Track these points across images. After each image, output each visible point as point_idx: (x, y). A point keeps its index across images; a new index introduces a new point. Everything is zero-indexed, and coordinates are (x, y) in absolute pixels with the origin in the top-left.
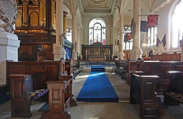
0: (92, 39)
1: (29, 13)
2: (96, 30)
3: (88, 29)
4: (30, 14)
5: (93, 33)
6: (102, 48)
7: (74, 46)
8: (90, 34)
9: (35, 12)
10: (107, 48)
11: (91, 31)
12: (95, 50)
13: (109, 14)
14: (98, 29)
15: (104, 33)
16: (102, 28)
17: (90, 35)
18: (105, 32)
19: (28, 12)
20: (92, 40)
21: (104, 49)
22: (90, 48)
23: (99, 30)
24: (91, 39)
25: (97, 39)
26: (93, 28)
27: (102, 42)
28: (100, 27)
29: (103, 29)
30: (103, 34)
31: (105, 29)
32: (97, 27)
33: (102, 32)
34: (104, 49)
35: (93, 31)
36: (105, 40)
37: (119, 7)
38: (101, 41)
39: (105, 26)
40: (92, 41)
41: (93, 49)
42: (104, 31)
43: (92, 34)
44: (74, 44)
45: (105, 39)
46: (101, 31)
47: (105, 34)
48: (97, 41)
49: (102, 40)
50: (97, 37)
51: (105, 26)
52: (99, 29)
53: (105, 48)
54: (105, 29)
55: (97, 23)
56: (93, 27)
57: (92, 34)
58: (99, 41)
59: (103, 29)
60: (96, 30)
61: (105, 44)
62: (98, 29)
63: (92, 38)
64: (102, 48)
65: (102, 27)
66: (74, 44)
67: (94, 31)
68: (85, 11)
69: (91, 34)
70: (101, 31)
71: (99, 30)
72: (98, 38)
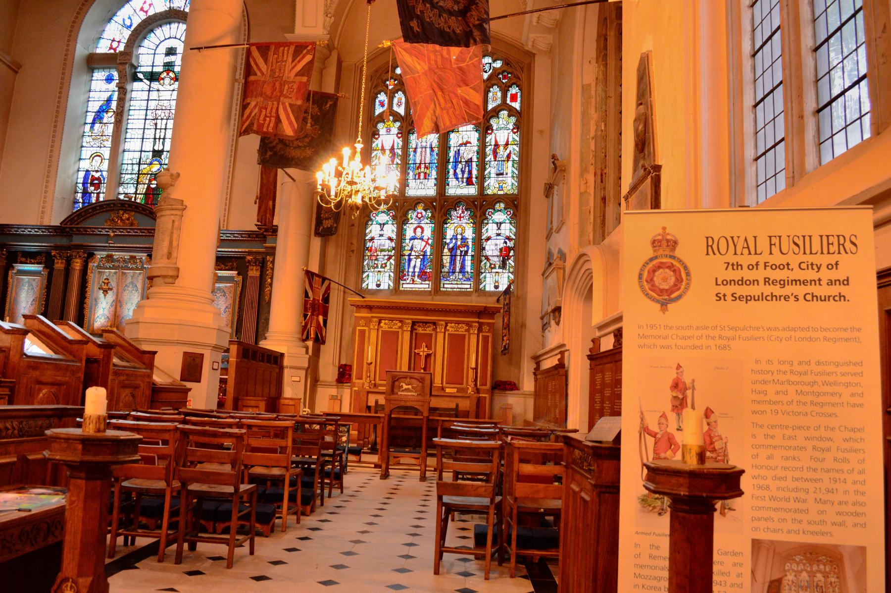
0: (105, 166)
2: (153, 77)
5: (114, 105)
14: (169, 67)
35: (122, 90)
63: (106, 153)
69: (98, 117)
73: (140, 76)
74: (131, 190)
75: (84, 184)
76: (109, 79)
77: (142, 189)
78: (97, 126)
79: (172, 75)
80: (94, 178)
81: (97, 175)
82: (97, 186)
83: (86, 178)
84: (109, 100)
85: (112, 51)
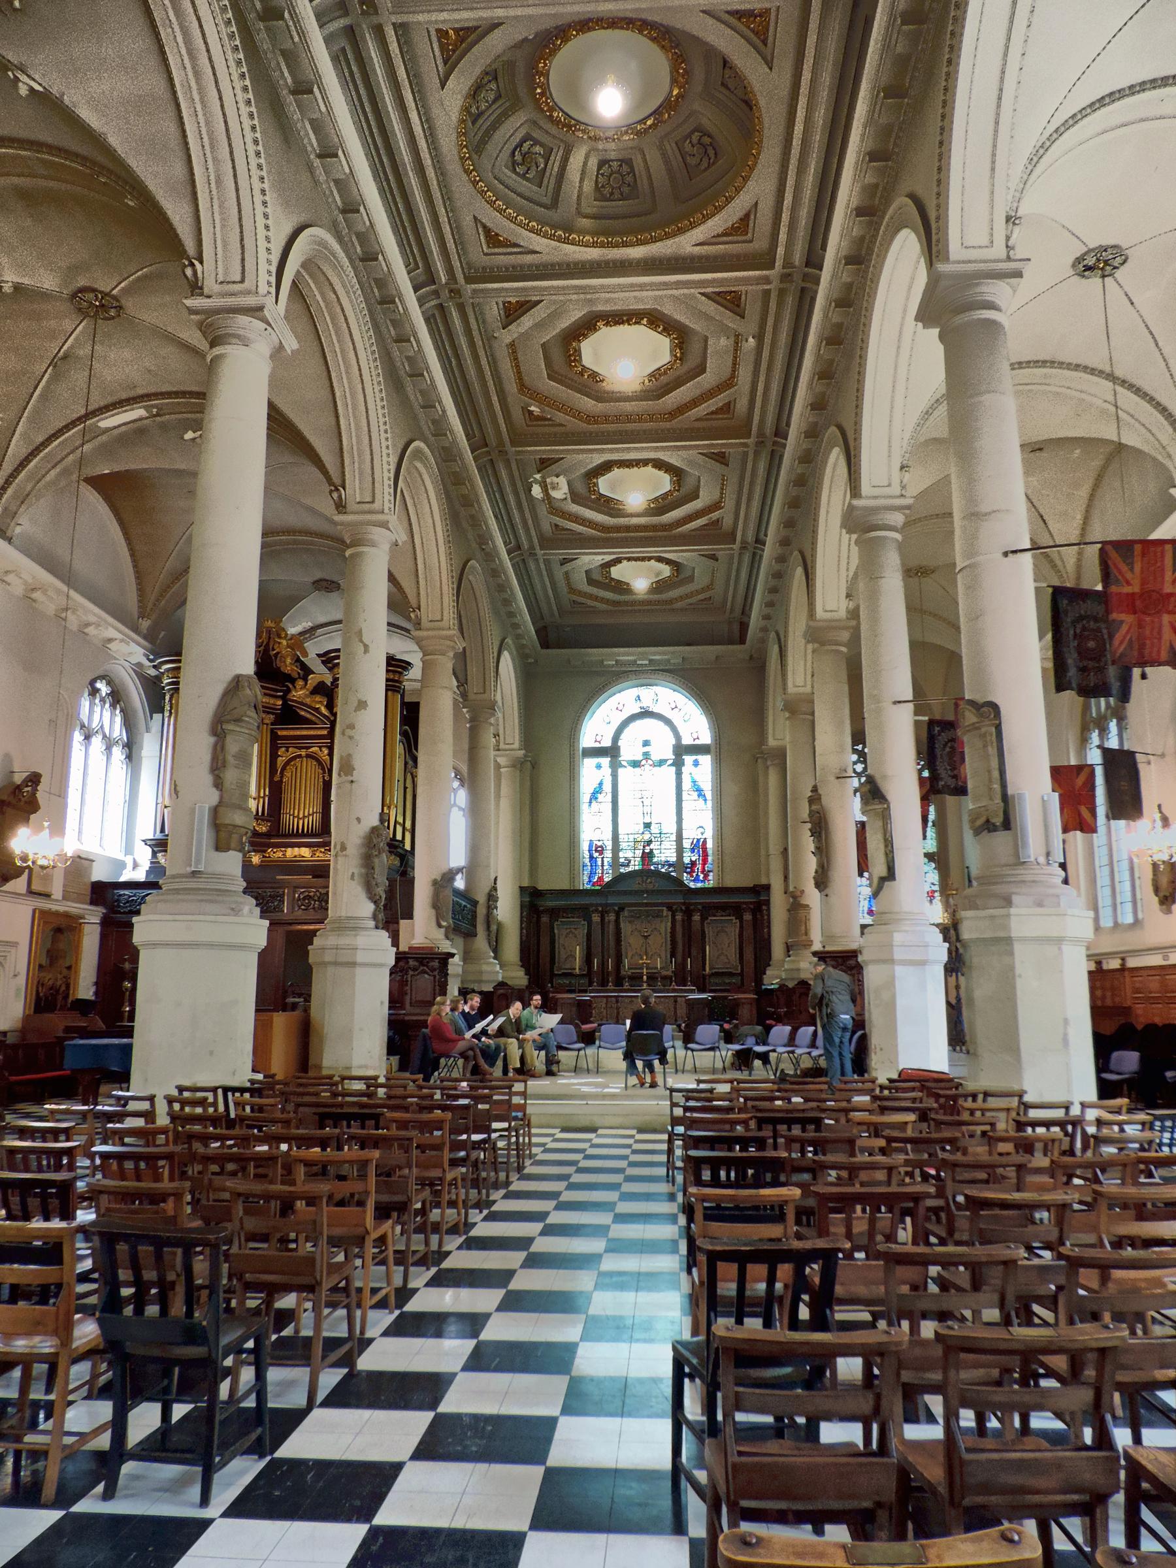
1: (280, 761)
2: (636, 764)
3: (572, 757)
4: (284, 769)
5: (607, 787)
6: (688, 913)
7: (481, 911)
8: (585, 797)
9: (308, 756)
10: (723, 908)
11: (591, 773)
12: (626, 927)
13: (736, 651)
14: (646, 755)
15: (700, 793)
16: (681, 751)
17: (584, 807)
18: (707, 784)
19: (274, 756)
20: (601, 850)
21: (703, 919)
22: (584, 912)
23: (661, 763)
24: (595, 836)
25: (647, 837)
26: (611, 752)
27: (686, 860)
28: (663, 747)
29: (688, 759)
30: (689, 797)
31: (706, 760)
32: (646, 743)
33: (687, 784)
34: (703, 919)
36: (710, 845)
37: (782, 637)
38: (680, 850)
39: (706, 738)
40: (608, 854)
41: (612, 917)
42: (702, 770)
43: (600, 797)
44: (481, 898)
45: (709, 834)
46: (679, 774)
47: (709, 795)
48: (647, 857)
49: (687, 844)
50: (647, 826)
51: (706, 738)
52: (655, 757)
53: (708, 910)
54: (706, 760)
55: (646, 714)
56: (607, 743)
57: (606, 798)
58: (665, 853)
59: (688, 759)
60: (636, 764)
61: (711, 883)
62: (646, 755)
64: (688, 913)
65: (687, 740)
66: (481, 898)
67: (621, 771)
68: (547, 637)
69: (594, 797)
70: (679, 774)
71: (661, 763)
72: (654, 829)
73: (624, 763)
74: (629, 854)
75: (590, 851)
76: (599, 767)
77: (639, 853)
78: (594, 802)
79: (650, 762)
80: (597, 847)
81: (599, 844)
82: (601, 853)
83: (590, 846)
84: (601, 784)
85: (597, 745)
